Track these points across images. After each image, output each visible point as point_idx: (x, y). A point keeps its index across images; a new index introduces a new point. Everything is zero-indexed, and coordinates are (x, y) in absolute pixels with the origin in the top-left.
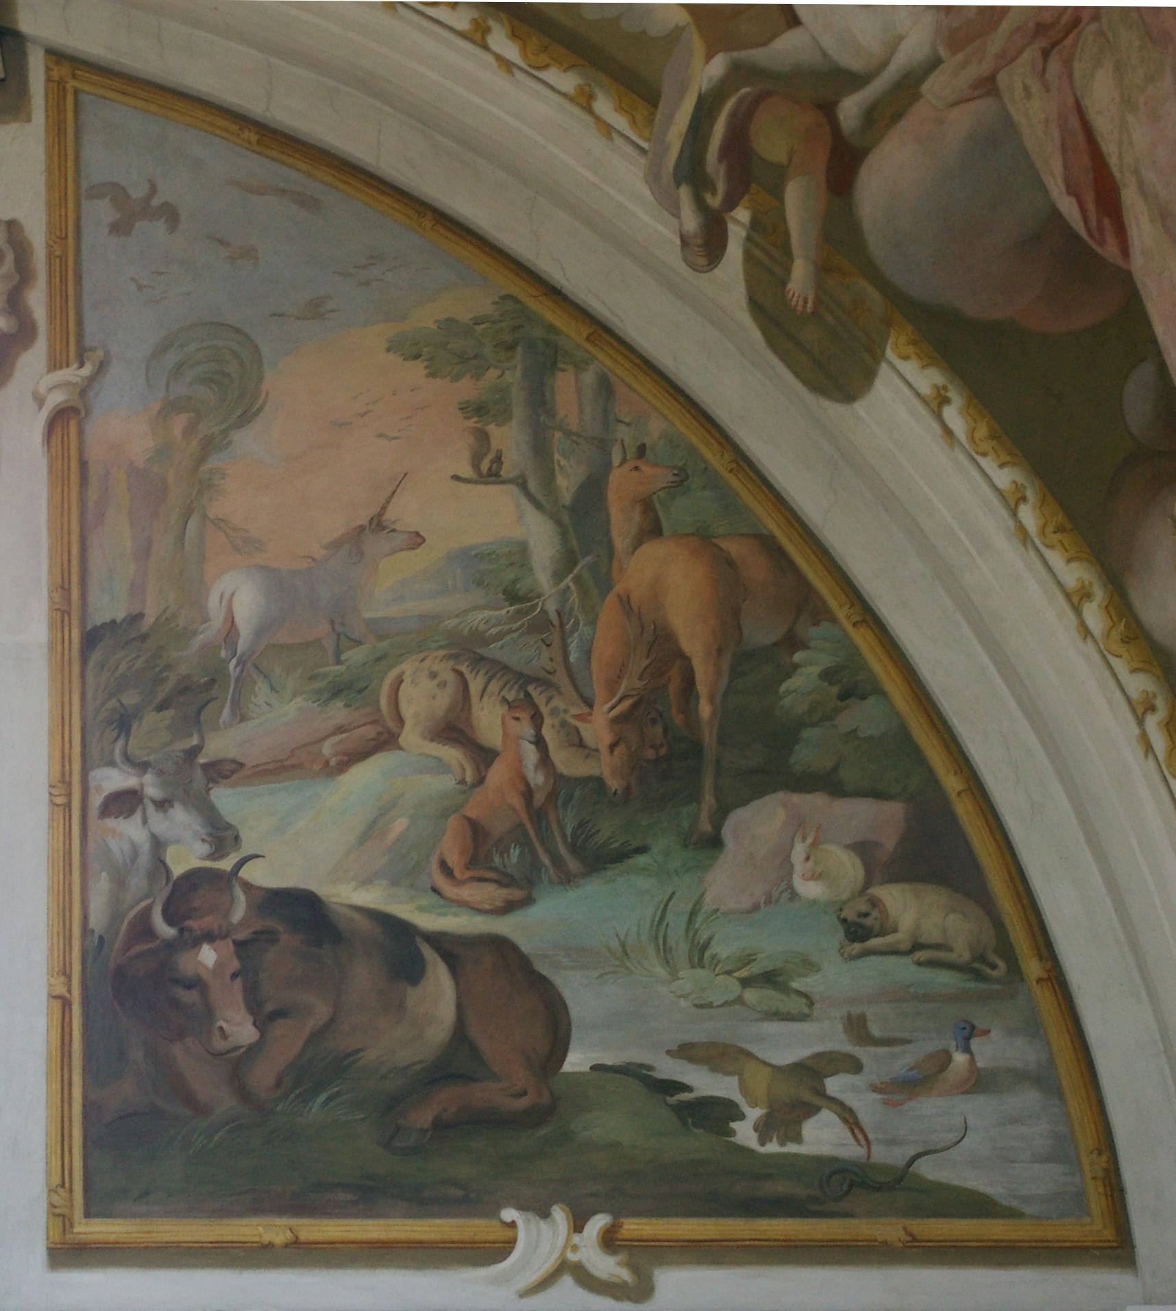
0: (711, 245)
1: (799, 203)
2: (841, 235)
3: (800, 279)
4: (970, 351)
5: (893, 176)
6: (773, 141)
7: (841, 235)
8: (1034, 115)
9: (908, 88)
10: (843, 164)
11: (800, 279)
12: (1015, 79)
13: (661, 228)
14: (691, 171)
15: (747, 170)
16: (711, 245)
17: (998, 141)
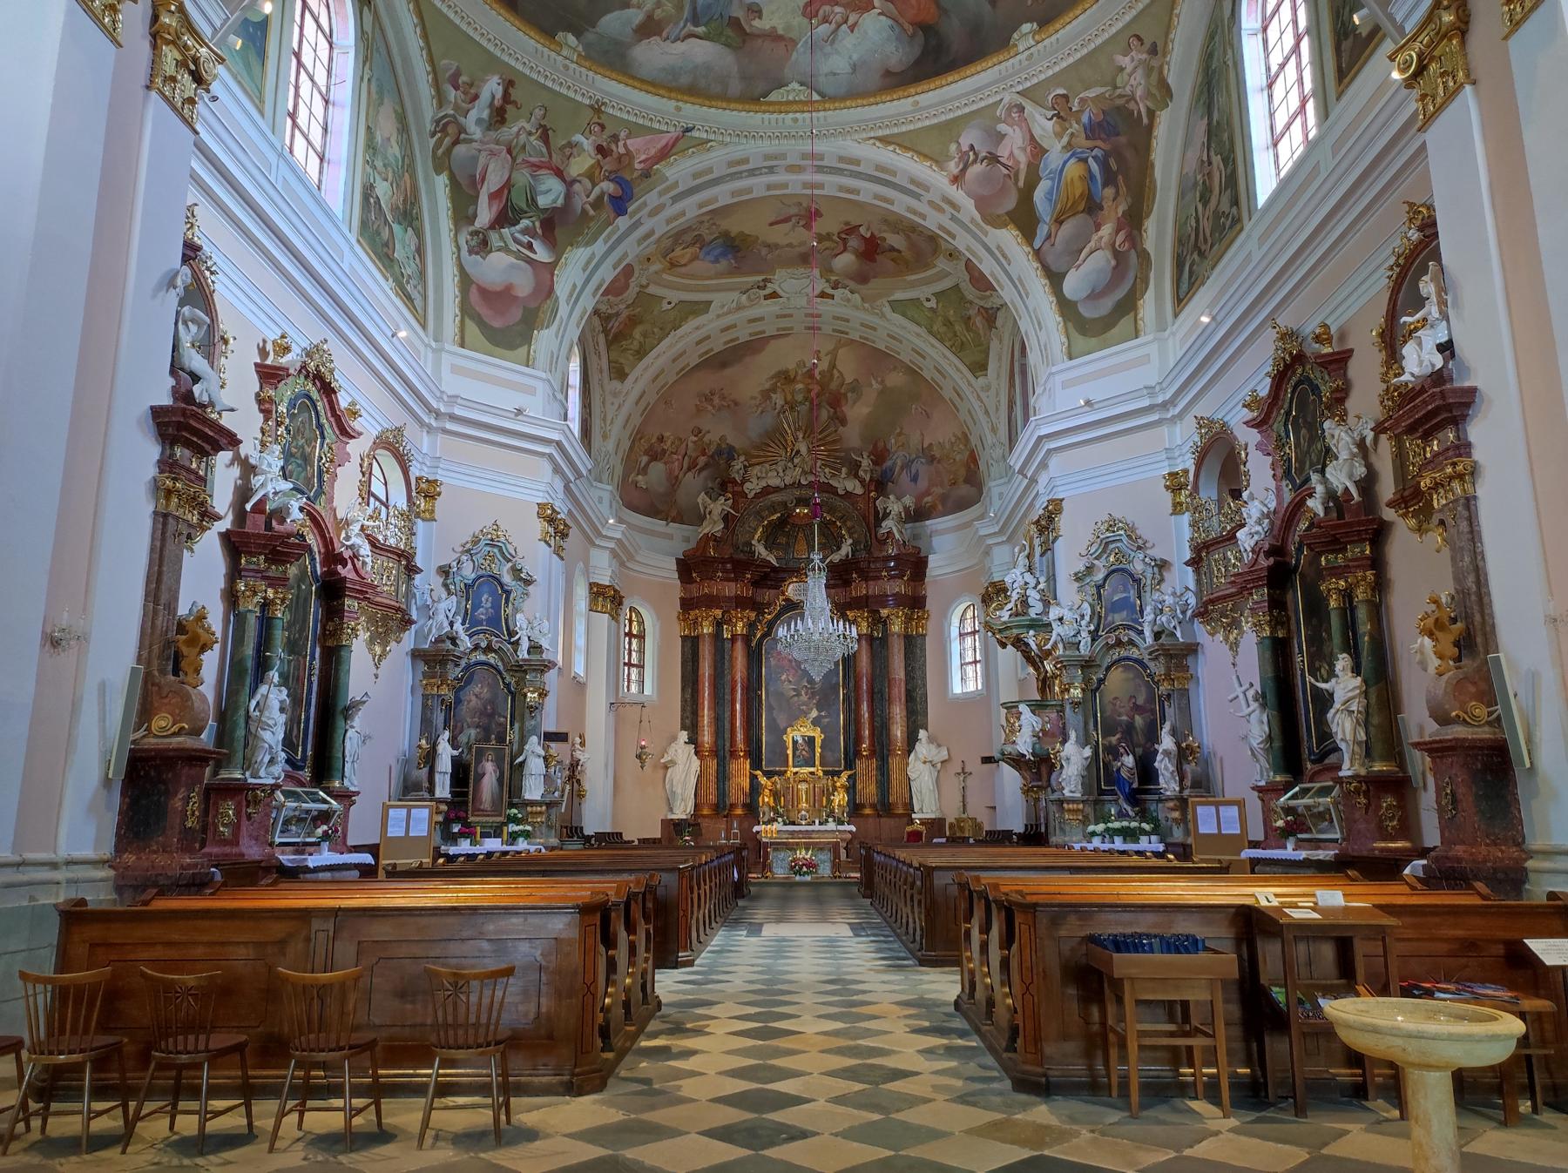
0: (433, 135)
1: (447, 141)
2: (449, 151)
3: (440, 152)
4: (454, 184)
5: (460, 149)
6: (451, 129)
7: (449, 151)
8: (482, 161)
9: (471, 141)
10: (456, 142)
11: (440, 152)
12: (484, 154)
13: (429, 127)
14: (438, 122)
15: (444, 130)
16: (433, 135)
17: (475, 159)
